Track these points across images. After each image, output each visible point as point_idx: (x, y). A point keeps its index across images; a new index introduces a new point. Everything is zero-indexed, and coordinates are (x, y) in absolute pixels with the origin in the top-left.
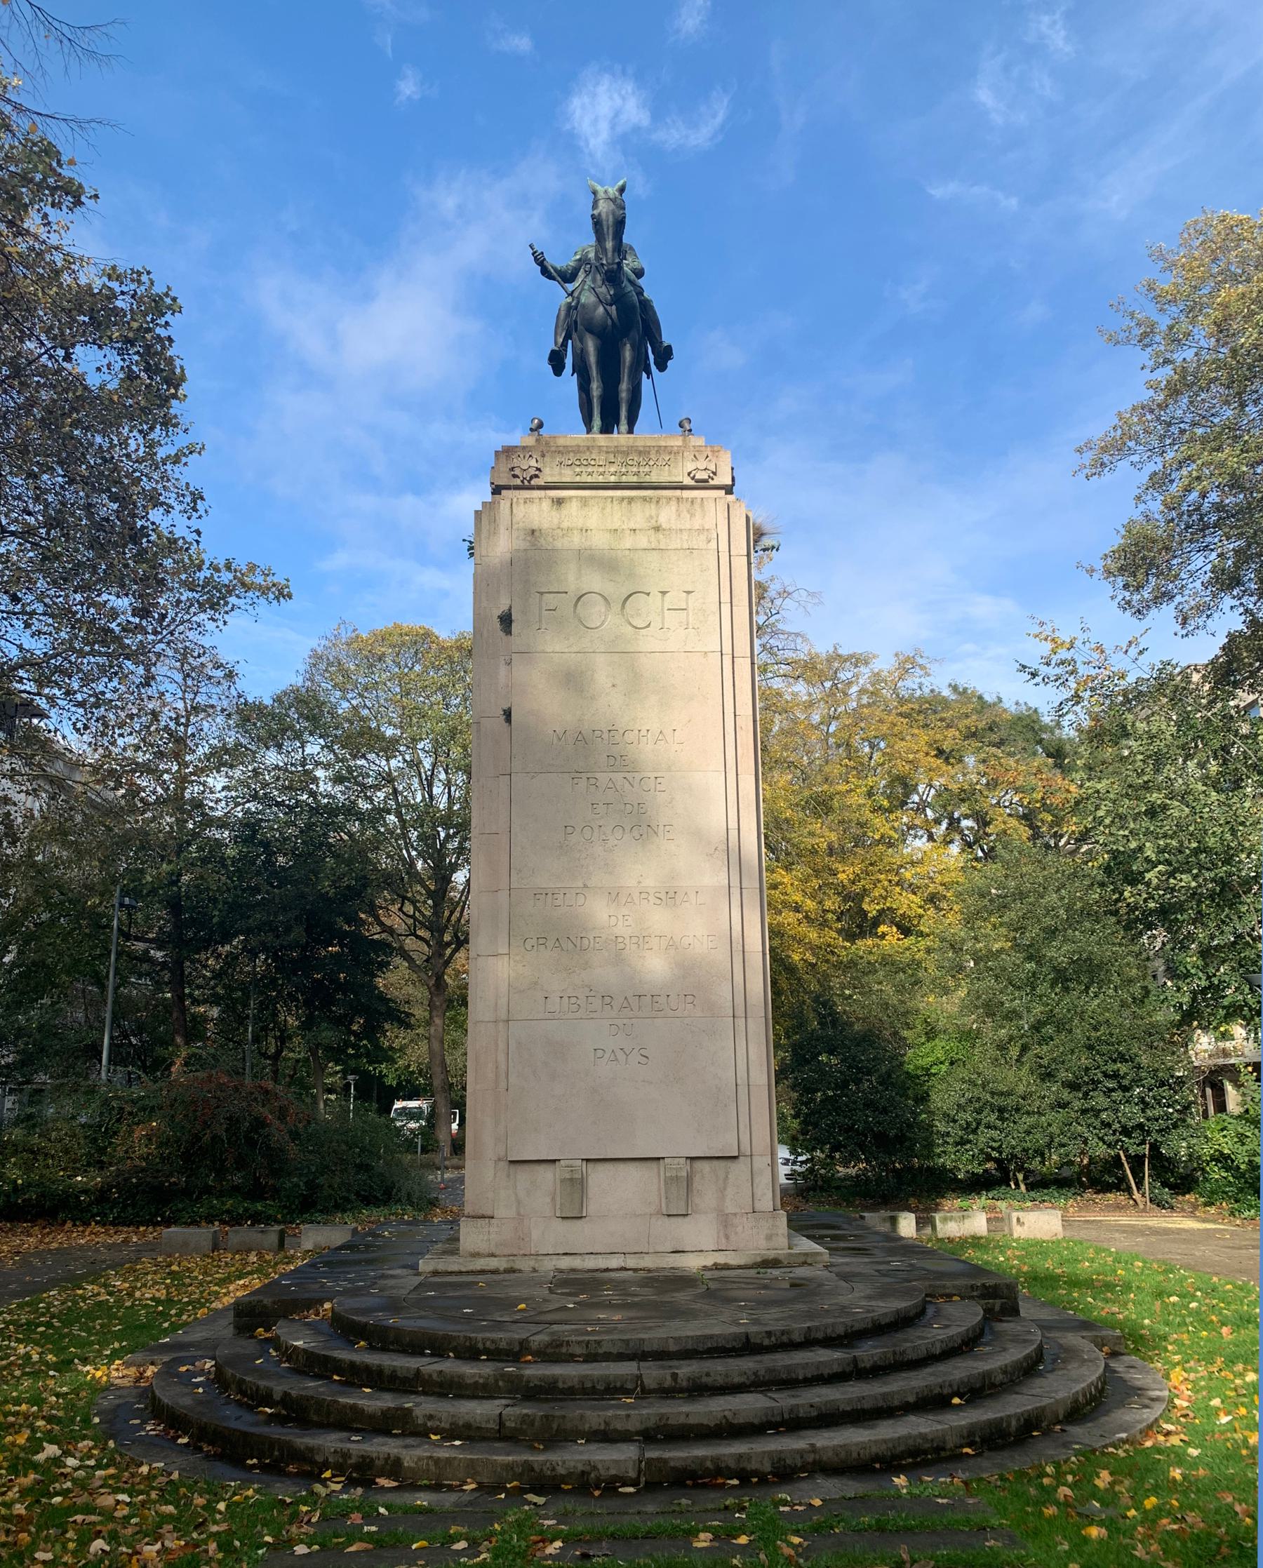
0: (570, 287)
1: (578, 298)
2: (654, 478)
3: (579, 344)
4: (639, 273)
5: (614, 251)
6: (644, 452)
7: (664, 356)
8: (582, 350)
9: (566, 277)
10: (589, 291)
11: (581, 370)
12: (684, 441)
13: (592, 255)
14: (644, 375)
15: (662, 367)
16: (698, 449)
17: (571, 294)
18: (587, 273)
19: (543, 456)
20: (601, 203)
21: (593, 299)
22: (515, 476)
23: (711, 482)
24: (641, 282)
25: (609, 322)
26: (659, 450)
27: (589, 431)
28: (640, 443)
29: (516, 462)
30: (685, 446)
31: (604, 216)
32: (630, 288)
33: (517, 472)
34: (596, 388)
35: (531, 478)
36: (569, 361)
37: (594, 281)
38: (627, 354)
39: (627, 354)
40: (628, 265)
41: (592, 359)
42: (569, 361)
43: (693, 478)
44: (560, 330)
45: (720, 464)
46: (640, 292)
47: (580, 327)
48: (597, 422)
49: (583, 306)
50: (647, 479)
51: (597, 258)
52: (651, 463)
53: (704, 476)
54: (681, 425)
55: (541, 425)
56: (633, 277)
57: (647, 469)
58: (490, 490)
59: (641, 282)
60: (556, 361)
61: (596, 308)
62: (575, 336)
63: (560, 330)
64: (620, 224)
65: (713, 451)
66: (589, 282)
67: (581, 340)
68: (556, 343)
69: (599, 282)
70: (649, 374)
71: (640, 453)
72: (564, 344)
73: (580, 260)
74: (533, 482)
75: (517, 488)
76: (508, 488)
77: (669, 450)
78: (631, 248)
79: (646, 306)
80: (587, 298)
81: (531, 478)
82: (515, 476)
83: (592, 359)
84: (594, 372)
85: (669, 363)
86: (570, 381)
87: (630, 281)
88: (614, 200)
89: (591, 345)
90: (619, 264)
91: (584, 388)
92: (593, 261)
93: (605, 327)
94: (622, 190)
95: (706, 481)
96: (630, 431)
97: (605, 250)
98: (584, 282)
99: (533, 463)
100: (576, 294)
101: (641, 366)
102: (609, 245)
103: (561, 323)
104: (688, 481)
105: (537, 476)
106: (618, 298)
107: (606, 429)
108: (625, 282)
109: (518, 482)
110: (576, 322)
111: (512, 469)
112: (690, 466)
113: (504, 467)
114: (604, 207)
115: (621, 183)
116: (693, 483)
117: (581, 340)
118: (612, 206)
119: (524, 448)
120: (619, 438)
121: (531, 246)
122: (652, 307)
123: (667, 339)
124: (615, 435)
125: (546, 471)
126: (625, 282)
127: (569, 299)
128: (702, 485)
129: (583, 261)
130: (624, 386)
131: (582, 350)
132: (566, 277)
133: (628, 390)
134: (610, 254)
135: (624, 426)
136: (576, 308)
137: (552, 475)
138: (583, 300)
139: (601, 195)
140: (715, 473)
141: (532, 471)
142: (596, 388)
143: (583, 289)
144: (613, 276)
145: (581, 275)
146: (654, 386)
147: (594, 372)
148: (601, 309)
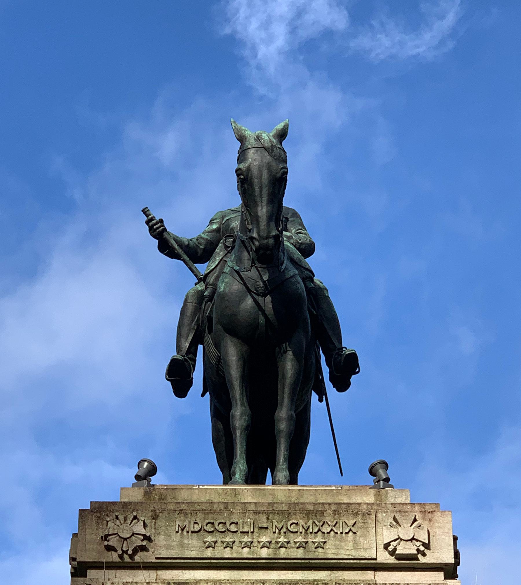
0: (202, 268)
1: (215, 286)
2: (331, 551)
3: (213, 348)
4: (308, 250)
5: (270, 219)
6: (315, 513)
7: (345, 368)
8: (219, 360)
9: (194, 253)
10: (232, 278)
11: (217, 387)
12: (378, 495)
13: (236, 224)
14: (314, 397)
15: (342, 385)
16: (400, 509)
17: (203, 279)
18: (229, 250)
19: (155, 517)
20: (251, 154)
21: (237, 286)
22: (110, 548)
23: (422, 560)
24: (311, 262)
25: (262, 320)
26: (339, 509)
27: (228, 479)
28: (308, 499)
29: (112, 527)
30: (379, 503)
31: (255, 171)
32: (293, 271)
33: (113, 541)
34: (239, 416)
35: (135, 551)
36: (198, 375)
37: (239, 260)
38: (289, 366)
39: (289, 366)
40: (290, 237)
41: (234, 372)
42: (198, 375)
43: (392, 553)
44: (185, 330)
45: (436, 531)
46: (308, 276)
47: (217, 327)
48: (240, 467)
49: (222, 296)
50: (320, 553)
51: (244, 229)
52: (326, 529)
53: (410, 549)
54: (372, 472)
55: (153, 470)
56: (297, 255)
57: (319, 538)
58: (68, 569)
59: (311, 262)
60: (179, 377)
61: (241, 300)
62: (208, 338)
63: (185, 330)
64: (279, 182)
65: (423, 512)
66: (231, 263)
67: (218, 346)
68: (179, 349)
69: (247, 263)
70: (322, 394)
71: (308, 514)
72: (192, 351)
73: (218, 230)
74: (137, 558)
75: (111, 566)
76: (98, 566)
77: (353, 509)
78: (295, 214)
79: (318, 297)
80: (229, 285)
81: (135, 551)
82: (110, 548)
83: (234, 372)
84: (237, 391)
85: (354, 379)
86: (198, 403)
87: (292, 260)
88: (269, 150)
89: (232, 353)
90: (278, 239)
91: (221, 413)
92: (238, 232)
93: (254, 326)
94: (282, 135)
95: (413, 557)
96: (293, 480)
97: (256, 219)
98: (223, 262)
99: (139, 528)
100: (211, 279)
101: (309, 382)
102: (263, 211)
103: (186, 321)
104: (384, 557)
105: (143, 549)
106: (278, 287)
107: (255, 477)
108: (286, 263)
109: (114, 557)
110: (210, 319)
111: (106, 538)
112: (387, 535)
113: (93, 535)
114: (253, 158)
115: (280, 126)
116: (392, 560)
117: (218, 346)
118: (268, 158)
119: (125, 505)
120: (275, 491)
121: (145, 212)
122: (327, 298)
123: (349, 342)
124: (269, 487)
125: (160, 540)
126: (286, 263)
127: (201, 287)
128: (408, 563)
129: (221, 233)
130: (283, 414)
131: (219, 360)
132: (194, 253)
133: (290, 418)
134: (263, 224)
135: (282, 474)
136: (211, 298)
137: (168, 547)
138: (222, 288)
139: (251, 142)
140: (427, 546)
141: (138, 542)
142: (239, 416)
143: (221, 272)
144: (268, 255)
145: (219, 253)
146: (331, 412)
147: (237, 391)
148: (249, 302)
